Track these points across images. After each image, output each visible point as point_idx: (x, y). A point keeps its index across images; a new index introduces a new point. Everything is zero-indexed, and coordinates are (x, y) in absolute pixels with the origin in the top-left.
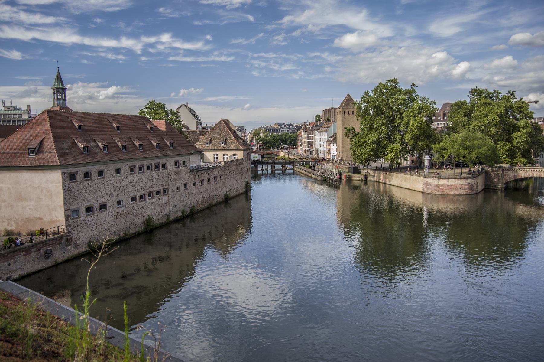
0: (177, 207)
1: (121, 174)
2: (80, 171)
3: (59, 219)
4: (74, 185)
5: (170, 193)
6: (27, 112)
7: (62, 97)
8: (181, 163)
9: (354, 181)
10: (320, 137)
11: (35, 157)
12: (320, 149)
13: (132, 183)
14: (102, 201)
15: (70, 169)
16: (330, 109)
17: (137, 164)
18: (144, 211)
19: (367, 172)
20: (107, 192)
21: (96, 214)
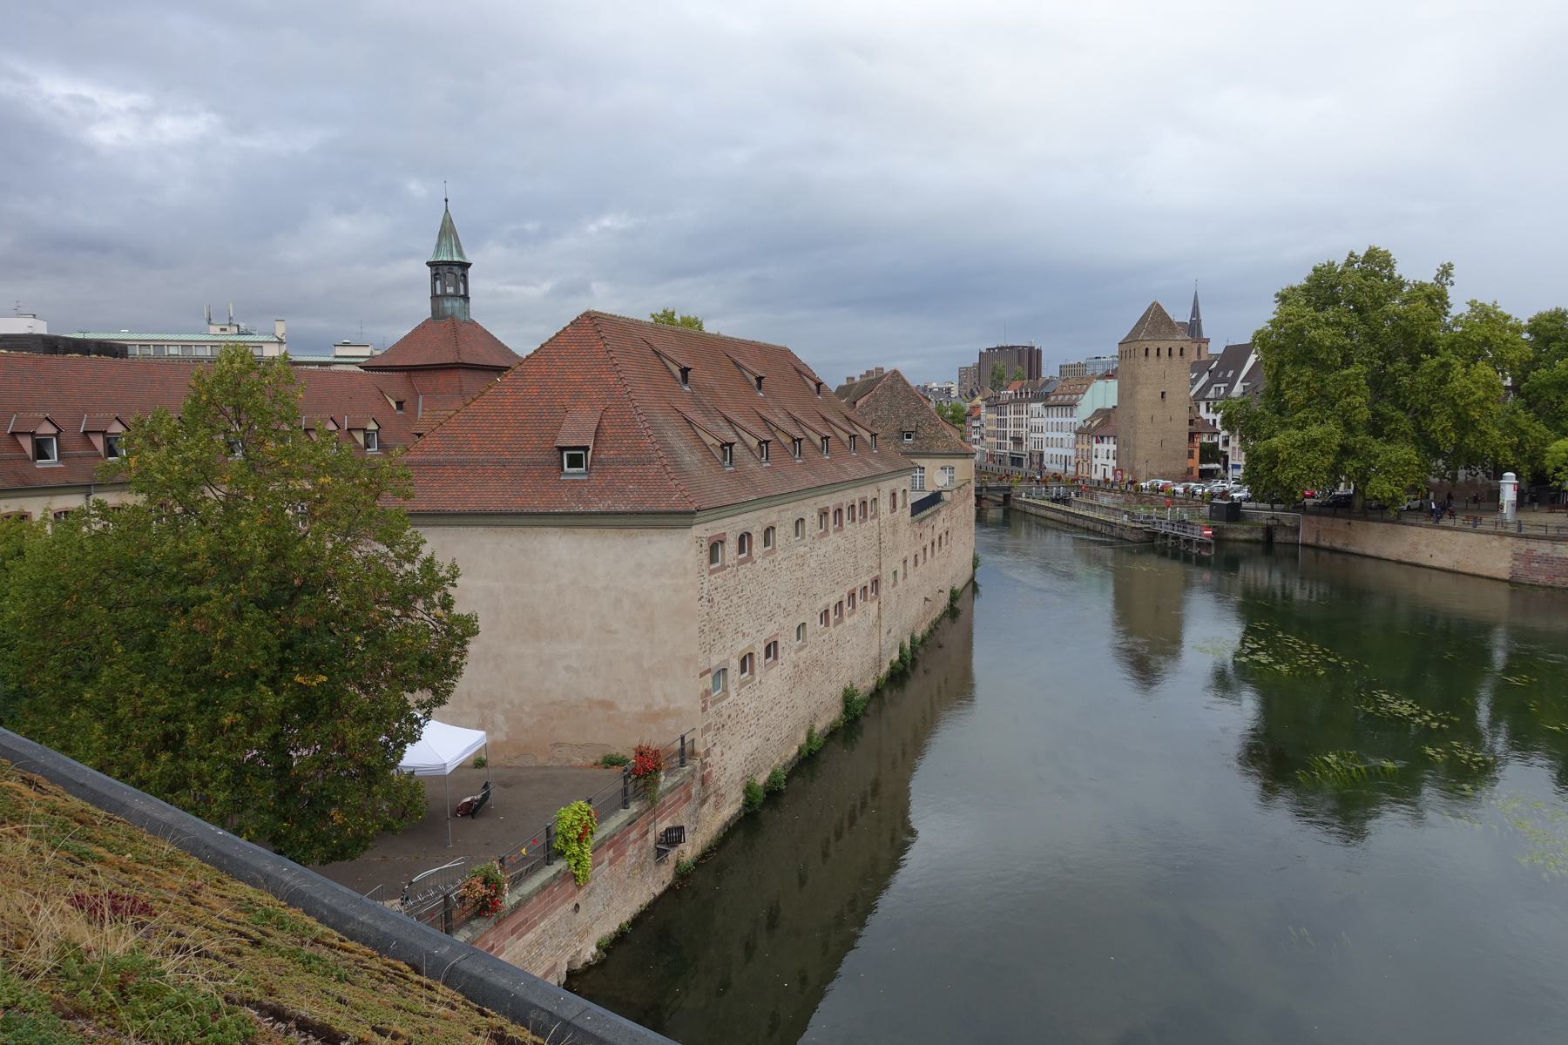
0: (892, 634)
1: (803, 538)
2: (730, 527)
3: (678, 705)
4: (719, 580)
5: (883, 592)
6: (276, 340)
7: (457, 289)
8: (899, 495)
9: (1230, 545)
10: (1050, 420)
11: (585, 477)
12: (1048, 451)
13: (823, 566)
14: (770, 630)
15: (715, 524)
16: (1001, 349)
17: (830, 501)
18: (840, 653)
19: (1273, 518)
20: (778, 601)
21: (758, 679)
